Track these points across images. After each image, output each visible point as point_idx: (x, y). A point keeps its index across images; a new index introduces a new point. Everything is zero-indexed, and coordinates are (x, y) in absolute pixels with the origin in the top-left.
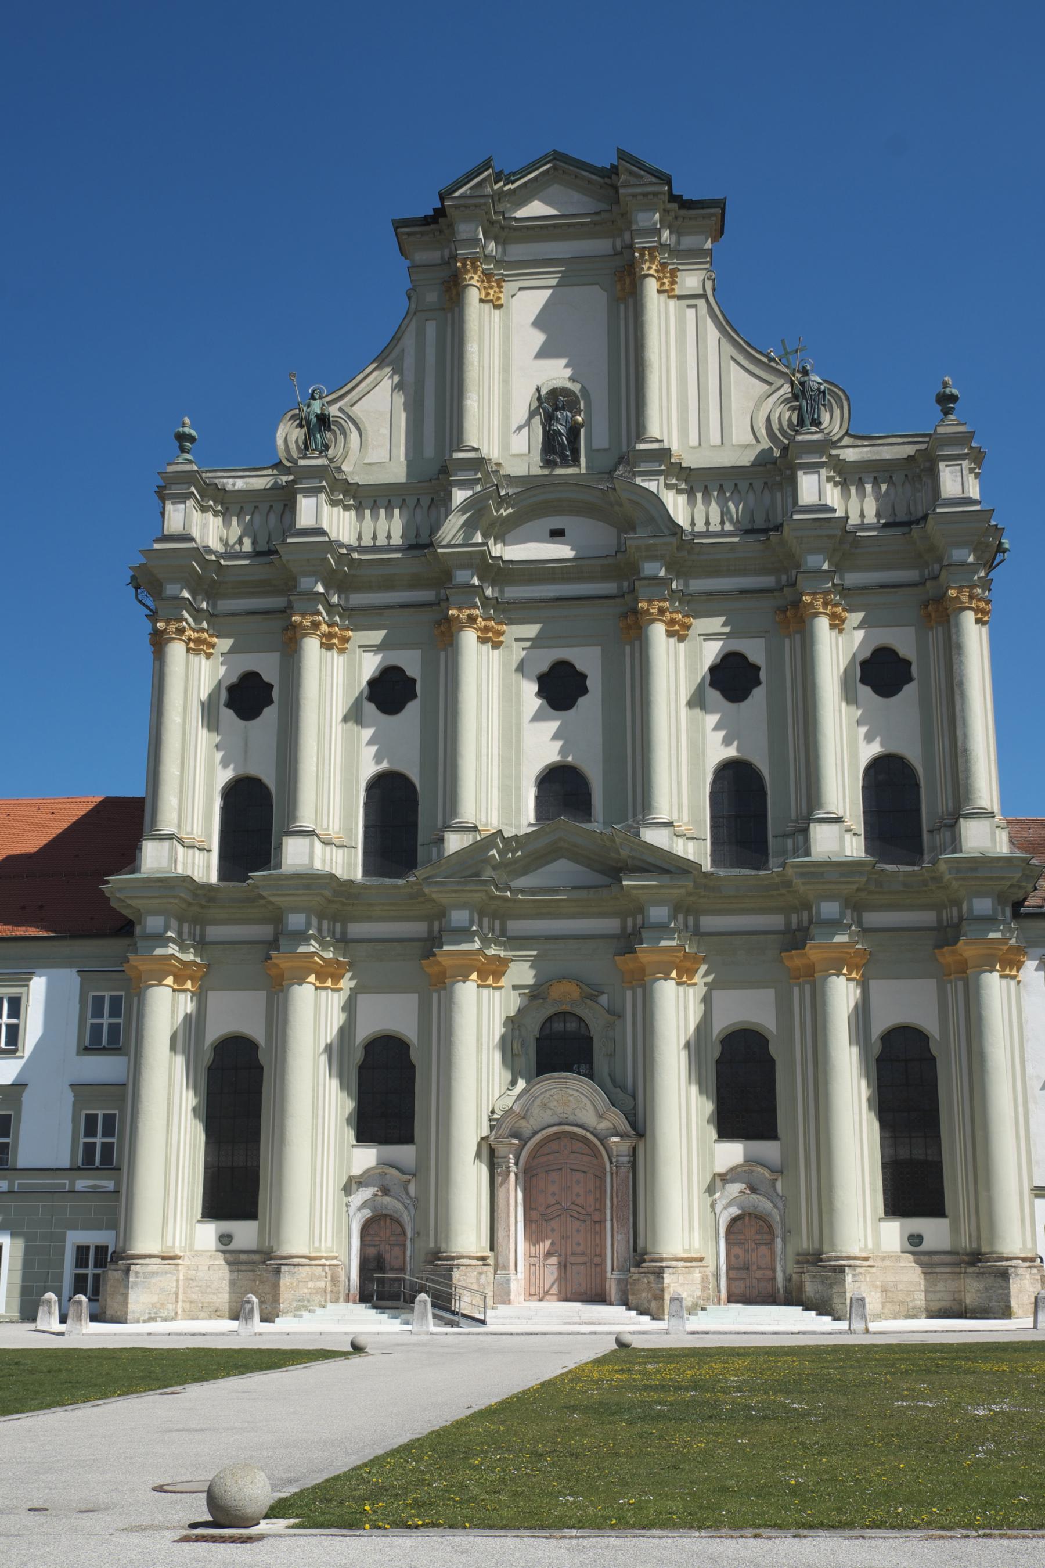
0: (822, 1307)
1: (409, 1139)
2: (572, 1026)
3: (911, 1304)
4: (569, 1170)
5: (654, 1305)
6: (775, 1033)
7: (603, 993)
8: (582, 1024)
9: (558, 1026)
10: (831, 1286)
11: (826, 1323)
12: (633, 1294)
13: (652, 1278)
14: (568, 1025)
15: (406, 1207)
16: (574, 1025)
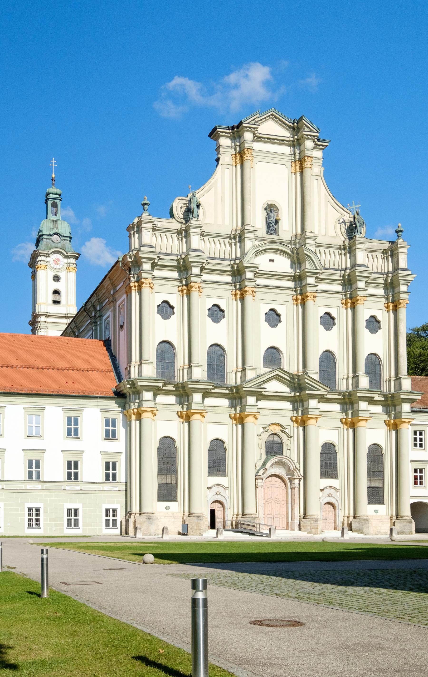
0: (360, 531)
1: (225, 475)
2: (276, 438)
3: (376, 531)
4: (274, 487)
5: (313, 530)
6: (338, 444)
7: (285, 428)
8: (279, 439)
9: (271, 439)
10: (363, 525)
11: (361, 536)
12: (303, 527)
13: (312, 522)
14: (274, 438)
15: (225, 498)
16: (276, 439)
